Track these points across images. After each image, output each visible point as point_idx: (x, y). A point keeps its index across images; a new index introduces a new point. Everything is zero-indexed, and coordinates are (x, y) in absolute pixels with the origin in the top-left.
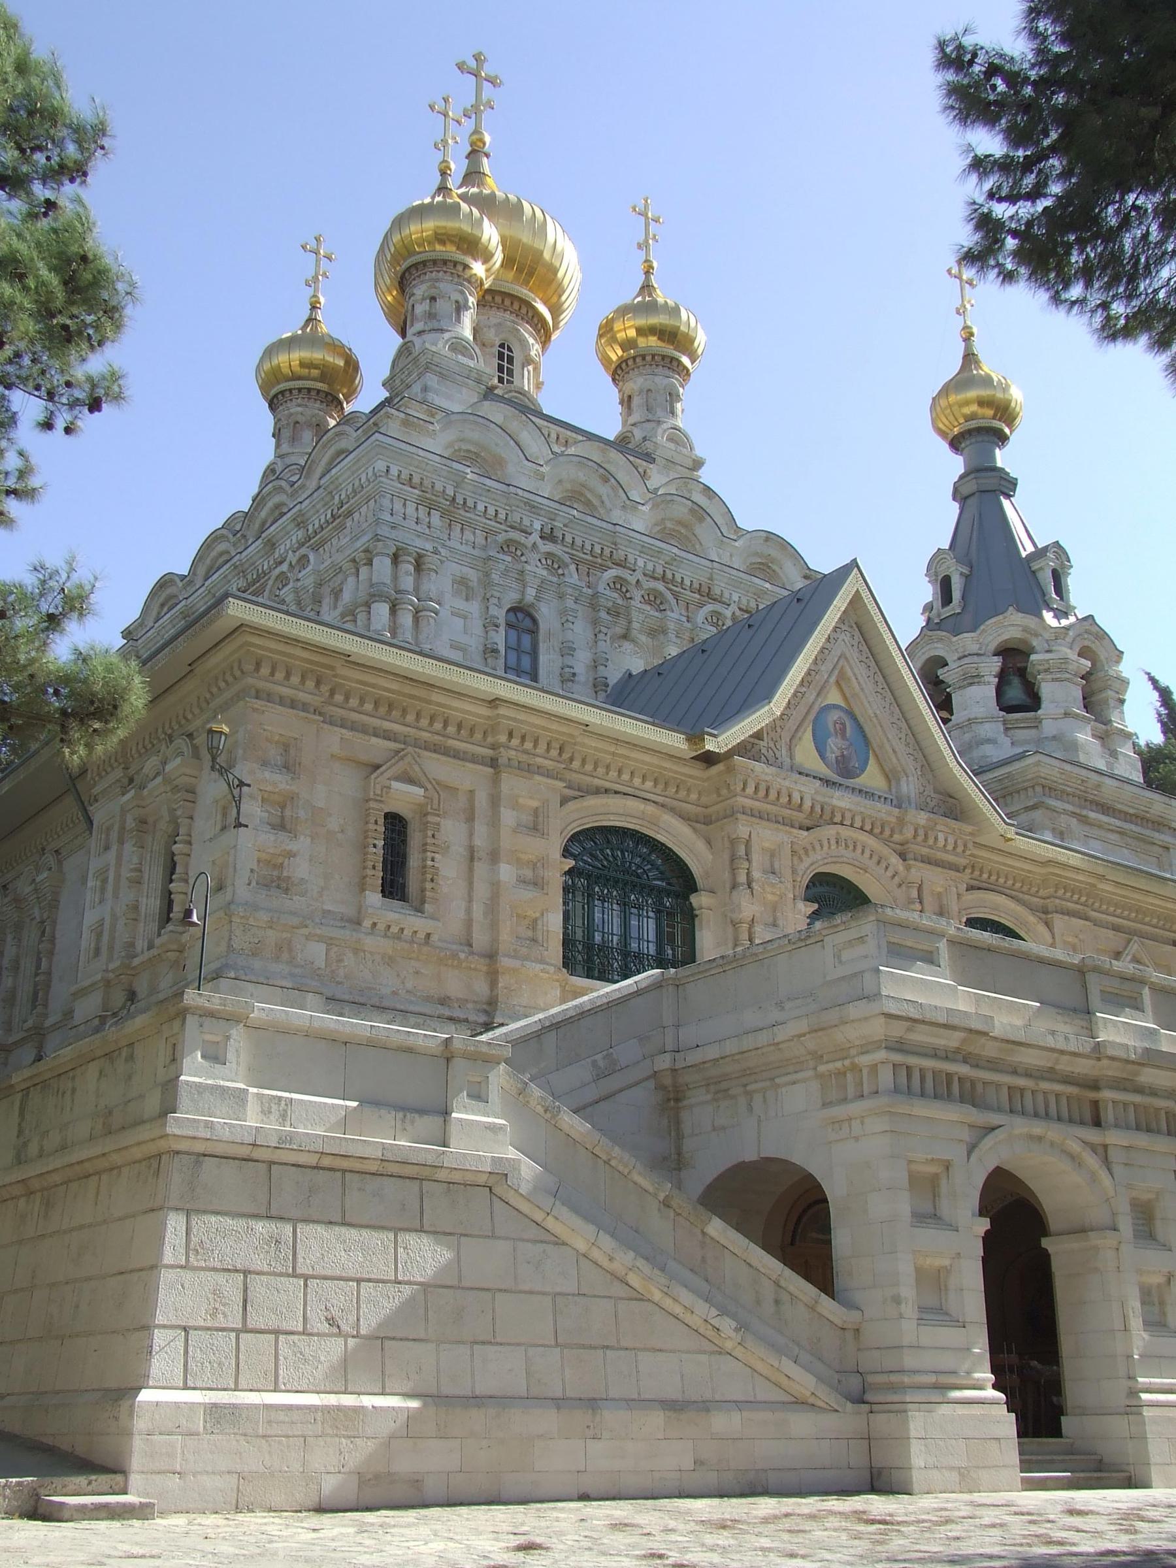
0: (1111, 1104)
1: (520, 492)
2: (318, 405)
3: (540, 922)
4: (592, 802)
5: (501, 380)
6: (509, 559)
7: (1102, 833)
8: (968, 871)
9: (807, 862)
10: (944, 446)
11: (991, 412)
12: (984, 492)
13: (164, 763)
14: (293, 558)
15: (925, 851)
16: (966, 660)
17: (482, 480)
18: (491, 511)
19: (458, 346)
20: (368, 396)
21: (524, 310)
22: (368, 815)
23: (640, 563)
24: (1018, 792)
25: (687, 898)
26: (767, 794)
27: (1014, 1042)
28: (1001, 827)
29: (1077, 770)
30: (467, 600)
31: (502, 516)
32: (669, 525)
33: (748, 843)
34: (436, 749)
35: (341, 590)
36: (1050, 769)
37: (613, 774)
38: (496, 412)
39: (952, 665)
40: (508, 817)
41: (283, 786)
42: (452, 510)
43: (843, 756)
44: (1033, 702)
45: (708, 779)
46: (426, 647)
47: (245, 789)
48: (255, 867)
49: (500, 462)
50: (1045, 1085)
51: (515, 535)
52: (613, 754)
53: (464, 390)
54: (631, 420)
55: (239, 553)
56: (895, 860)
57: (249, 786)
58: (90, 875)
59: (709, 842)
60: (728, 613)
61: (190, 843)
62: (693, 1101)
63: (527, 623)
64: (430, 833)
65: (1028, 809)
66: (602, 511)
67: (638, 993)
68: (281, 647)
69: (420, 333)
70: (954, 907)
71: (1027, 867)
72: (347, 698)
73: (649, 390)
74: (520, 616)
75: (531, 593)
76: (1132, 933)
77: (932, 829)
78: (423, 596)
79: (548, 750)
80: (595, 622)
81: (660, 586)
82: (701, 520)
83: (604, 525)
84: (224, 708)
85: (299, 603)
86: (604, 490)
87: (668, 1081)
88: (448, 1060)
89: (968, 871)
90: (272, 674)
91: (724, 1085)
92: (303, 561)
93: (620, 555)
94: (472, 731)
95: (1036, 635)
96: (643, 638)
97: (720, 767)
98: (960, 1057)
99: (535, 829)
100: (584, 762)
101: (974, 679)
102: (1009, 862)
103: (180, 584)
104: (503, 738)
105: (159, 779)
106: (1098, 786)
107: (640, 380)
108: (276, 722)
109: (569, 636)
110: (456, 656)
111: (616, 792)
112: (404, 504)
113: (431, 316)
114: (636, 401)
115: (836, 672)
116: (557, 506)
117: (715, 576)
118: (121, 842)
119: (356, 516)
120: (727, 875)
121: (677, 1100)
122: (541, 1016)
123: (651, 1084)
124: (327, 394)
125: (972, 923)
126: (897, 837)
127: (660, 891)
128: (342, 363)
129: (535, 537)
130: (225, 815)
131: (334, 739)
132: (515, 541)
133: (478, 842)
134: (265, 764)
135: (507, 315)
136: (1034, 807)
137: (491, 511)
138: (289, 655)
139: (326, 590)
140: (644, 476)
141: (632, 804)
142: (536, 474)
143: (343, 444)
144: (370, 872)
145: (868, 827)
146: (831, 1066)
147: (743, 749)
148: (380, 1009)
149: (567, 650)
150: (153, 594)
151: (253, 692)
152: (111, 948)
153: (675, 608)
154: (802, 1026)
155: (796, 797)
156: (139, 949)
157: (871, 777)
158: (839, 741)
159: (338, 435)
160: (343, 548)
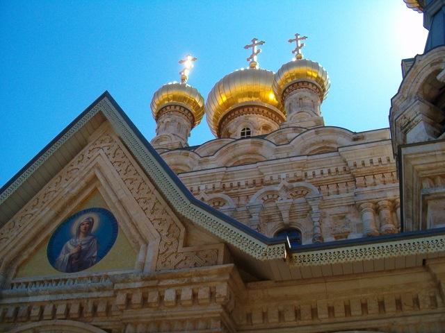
32: (241, 158)
71: (401, 279)
81: (219, 195)
82: (261, 145)
102: (363, 283)
117: (262, 171)
158: (81, 240)
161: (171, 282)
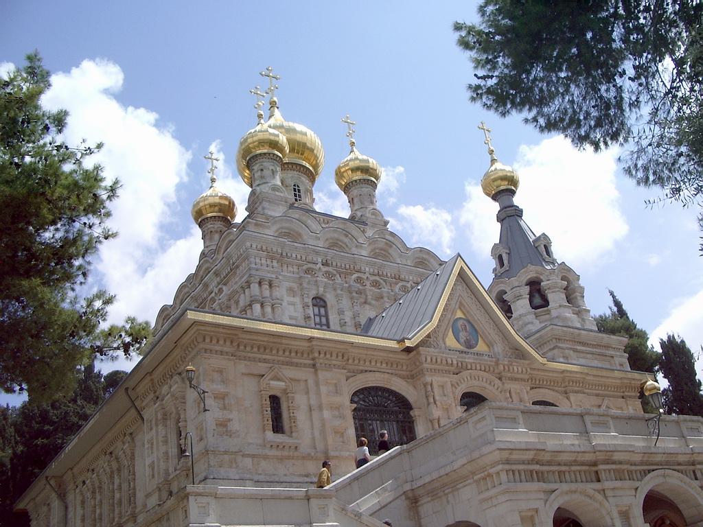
0: (603, 472)
1: (310, 247)
2: (219, 222)
3: (345, 434)
4: (360, 376)
5: (296, 200)
6: (309, 276)
7: (585, 355)
8: (530, 381)
9: (459, 388)
10: (490, 199)
11: (507, 183)
12: (510, 216)
13: (170, 387)
14: (216, 290)
15: (509, 375)
16: (514, 290)
17: (292, 244)
18: (299, 257)
19: (275, 188)
20: (241, 215)
21: (302, 169)
22: (262, 397)
23: (367, 269)
24: (549, 341)
25: (409, 413)
26: (436, 362)
27: (557, 452)
28: (541, 360)
29: (569, 329)
30: (294, 297)
31: (304, 258)
32: (377, 251)
33: (431, 385)
34: (288, 364)
35: (239, 301)
36: (558, 331)
37: (367, 363)
38: (296, 214)
39: (509, 293)
40: (324, 389)
41: (222, 390)
42: (282, 258)
43: (467, 340)
44: (546, 303)
45: (410, 359)
46: (279, 320)
47: (206, 394)
48: (215, 428)
49: (300, 235)
50: (574, 468)
51: (310, 266)
52: (366, 354)
53: (281, 207)
54: (355, 209)
55: (193, 291)
56: (497, 381)
57: (207, 392)
58: (146, 442)
59: (415, 387)
60: (409, 285)
61: (186, 421)
62: (423, 502)
63: (322, 303)
64: (290, 401)
65: (551, 350)
66: (347, 249)
67: (392, 458)
68: (213, 329)
69: (258, 185)
70: (526, 398)
71: (555, 375)
72: (245, 347)
73: (360, 195)
74: (318, 300)
75: (321, 289)
76: (604, 396)
77: (511, 365)
78: (274, 298)
79: (337, 357)
80: (352, 298)
82: (391, 247)
83: (349, 255)
84: (192, 360)
85: (221, 309)
86: (346, 240)
87: (410, 495)
88: (308, 500)
89: (530, 381)
90: (211, 341)
91: (435, 493)
92: (221, 291)
93: (357, 267)
94: (302, 354)
95: (541, 274)
96: (373, 302)
97: (415, 352)
98: (535, 462)
99: (336, 393)
100: (354, 360)
101: (519, 297)
103: (170, 309)
104: (316, 355)
105: (169, 395)
106: (579, 335)
107: (356, 191)
108: (215, 361)
109: (341, 306)
110: (293, 322)
111: (371, 371)
112: (261, 260)
113: (262, 177)
114: (355, 201)
115: (458, 303)
116: (327, 250)
118: (157, 425)
119: (241, 268)
120: (425, 400)
121: (416, 503)
122: (349, 475)
123: (403, 497)
124: (223, 217)
125: (534, 403)
126: (496, 371)
127: (396, 412)
128: (227, 203)
129: (320, 265)
130: (199, 407)
131: (242, 367)
132: (310, 268)
133: (312, 402)
134: (212, 381)
135: (295, 172)
136: (554, 348)
137: (299, 257)
138: (218, 332)
139: (232, 301)
140: (364, 232)
141: (377, 374)
142: (315, 239)
143: (231, 237)
144: (266, 422)
145: (483, 369)
146: (479, 476)
147: (423, 343)
148: (280, 483)
149: (341, 312)
150: (159, 316)
151: (203, 351)
152: (159, 473)
153: (385, 286)
154: (464, 461)
155: (450, 361)
156: (170, 472)
157: (481, 347)
158: (464, 333)
159: (228, 234)
160: (236, 282)
161: (516, 364)
